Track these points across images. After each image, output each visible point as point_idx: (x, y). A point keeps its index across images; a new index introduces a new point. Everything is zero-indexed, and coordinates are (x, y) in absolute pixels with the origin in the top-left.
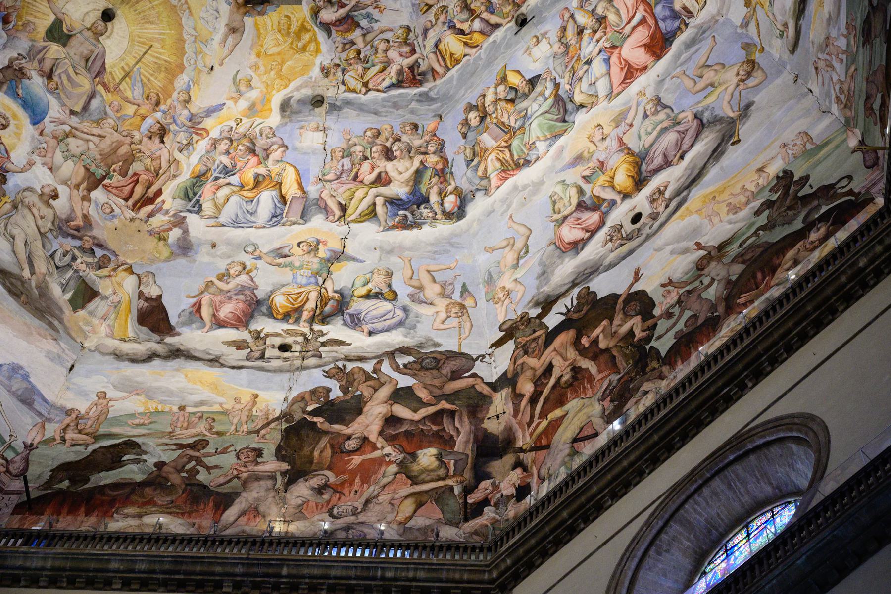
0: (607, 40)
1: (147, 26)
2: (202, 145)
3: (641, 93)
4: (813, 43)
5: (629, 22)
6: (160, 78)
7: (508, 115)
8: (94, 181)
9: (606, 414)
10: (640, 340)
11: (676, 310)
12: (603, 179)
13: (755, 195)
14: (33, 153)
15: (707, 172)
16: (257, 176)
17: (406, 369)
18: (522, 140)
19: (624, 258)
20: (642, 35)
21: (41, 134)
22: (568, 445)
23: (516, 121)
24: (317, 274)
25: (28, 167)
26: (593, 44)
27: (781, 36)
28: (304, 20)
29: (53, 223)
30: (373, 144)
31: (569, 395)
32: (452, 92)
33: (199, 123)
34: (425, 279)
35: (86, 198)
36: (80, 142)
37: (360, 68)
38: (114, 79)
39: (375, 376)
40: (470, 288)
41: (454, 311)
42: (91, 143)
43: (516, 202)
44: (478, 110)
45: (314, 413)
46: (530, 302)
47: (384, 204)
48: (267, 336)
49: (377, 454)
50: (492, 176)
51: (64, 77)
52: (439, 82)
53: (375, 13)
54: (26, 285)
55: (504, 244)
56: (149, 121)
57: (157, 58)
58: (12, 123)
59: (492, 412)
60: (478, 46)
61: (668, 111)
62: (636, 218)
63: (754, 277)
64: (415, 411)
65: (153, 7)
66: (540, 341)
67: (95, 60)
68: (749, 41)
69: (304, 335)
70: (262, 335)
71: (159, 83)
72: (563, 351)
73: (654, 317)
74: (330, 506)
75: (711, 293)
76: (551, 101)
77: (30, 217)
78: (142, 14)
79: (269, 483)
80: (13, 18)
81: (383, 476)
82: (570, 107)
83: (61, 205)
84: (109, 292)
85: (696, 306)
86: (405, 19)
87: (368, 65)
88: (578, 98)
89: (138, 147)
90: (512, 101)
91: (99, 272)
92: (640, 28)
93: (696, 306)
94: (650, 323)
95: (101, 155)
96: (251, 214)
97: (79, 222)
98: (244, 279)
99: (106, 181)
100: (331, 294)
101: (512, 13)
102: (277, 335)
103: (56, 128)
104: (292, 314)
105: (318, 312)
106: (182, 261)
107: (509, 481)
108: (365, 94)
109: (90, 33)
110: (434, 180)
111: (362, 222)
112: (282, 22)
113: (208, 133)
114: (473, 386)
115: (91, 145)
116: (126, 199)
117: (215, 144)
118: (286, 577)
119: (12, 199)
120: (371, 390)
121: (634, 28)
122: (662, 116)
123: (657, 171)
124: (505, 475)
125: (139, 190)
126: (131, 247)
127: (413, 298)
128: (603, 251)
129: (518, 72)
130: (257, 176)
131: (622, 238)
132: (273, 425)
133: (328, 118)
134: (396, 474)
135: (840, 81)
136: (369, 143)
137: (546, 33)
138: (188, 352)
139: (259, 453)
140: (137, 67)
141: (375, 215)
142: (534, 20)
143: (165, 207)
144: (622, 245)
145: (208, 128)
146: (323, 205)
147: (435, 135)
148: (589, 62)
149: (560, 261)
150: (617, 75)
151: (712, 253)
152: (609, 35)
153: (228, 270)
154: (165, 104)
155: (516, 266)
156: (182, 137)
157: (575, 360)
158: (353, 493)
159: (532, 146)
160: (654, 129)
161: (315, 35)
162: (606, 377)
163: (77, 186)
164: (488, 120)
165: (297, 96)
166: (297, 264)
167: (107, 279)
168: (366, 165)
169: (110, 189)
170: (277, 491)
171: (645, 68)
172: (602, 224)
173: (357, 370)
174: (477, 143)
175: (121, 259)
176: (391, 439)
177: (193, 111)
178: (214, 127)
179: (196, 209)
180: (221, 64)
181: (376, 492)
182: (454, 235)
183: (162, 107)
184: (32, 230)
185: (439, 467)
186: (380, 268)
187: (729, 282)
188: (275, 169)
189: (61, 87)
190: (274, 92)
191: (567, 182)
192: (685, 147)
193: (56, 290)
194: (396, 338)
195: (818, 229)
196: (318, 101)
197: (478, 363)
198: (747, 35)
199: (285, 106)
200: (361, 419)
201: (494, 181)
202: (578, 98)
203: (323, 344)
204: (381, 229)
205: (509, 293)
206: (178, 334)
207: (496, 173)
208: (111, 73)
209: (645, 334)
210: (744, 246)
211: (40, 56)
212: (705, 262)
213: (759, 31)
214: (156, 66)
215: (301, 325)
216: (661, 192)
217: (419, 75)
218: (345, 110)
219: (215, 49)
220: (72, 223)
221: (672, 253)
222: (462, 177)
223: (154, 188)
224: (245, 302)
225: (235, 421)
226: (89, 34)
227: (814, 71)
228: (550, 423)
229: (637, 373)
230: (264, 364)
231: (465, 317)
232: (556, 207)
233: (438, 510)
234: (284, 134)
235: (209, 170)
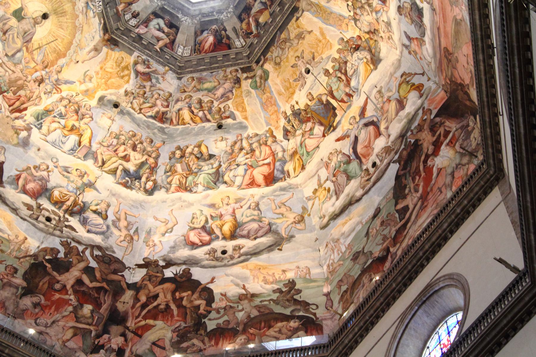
0: (251, 161)
1: (60, 29)
3: (253, 196)
4: (331, 235)
5: (263, 160)
7: (194, 165)
9: (173, 341)
10: (201, 314)
11: (222, 311)
12: (219, 222)
13: (276, 282)
15: (263, 254)
16: (73, 126)
17: (96, 258)
18: (194, 179)
19: (211, 267)
20: (265, 170)
22: (150, 344)
23: (195, 168)
24: (78, 188)
26: (244, 158)
27: (320, 218)
28: (129, 64)
30: (130, 139)
31: (160, 317)
32: (175, 135)
33: (60, 85)
34: (123, 216)
36: (3, 70)
37: (142, 100)
38: (33, 47)
39: (82, 254)
40: (139, 231)
41: (128, 238)
42: (7, 73)
43: (178, 205)
44: (182, 152)
45: (48, 261)
46: (161, 257)
47: (122, 171)
48: (44, 209)
49: (67, 297)
50: (173, 185)
51: (11, 36)
52: (171, 127)
53: (161, 79)
55: (164, 220)
57: (57, 46)
59: (122, 300)
60: (196, 123)
61: (259, 212)
62: (224, 252)
63: (261, 324)
64: (91, 282)
66: (158, 279)
68: (306, 207)
69: (60, 217)
70: (41, 207)
71: (51, 58)
72: (166, 292)
73: (211, 307)
74: (37, 317)
75: (240, 315)
76: (214, 170)
79: (15, 290)
81: (65, 311)
82: (221, 179)
85: (231, 318)
86: (171, 90)
87: (146, 101)
88: (226, 178)
89: (27, 83)
90: (198, 158)
92: (266, 166)
93: (231, 318)
94: (209, 308)
96: (63, 143)
98: (45, 174)
99: (5, 94)
100: (80, 202)
101: (218, 120)
102: (48, 211)
104: (58, 203)
105: (70, 208)
106: (21, 150)
107: (116, 342)
108: (138, 114)
110: (148, 171)
111: (109, 174)
113: (61, 91)
114: (120, 281)
116: (10, 106)
117: (62, 99)
118: (6, 354)
120: (77, 261)
121: (264, 164)
122: (256, 213)
123: (243, 237)
124: (116, 336)
125: (18, 104)
127: (113, 222)
128: (203, 257)
129: (207, 148)
130: (73, 126)
131: (214, 257)
132: (28, 258)
133: (117, 116)
134: (71, 312)
135: (333, 260)
136: (129, 138)
137: (227, 139)
138: (5, 198)
139: (16, 271)
141: (116, 174)
142: (225, 130)
143: (25, 118)
144: (213, 260)
145: (62, 90)
146: (95, 156)
147: (158, 150)
148: (238, 165)
149: (183, 247)
150: (247, 181)
151: (248, 296)
152: (252, 160)
153: (40, 165)
155: (163, 235)
156: (49, 88)
157: (169, 301)
158: (49, 314)
159: (196, 185)
160: (250, 216)
161: (130, 73)
162: (180, 321)
164: (184, 159)
165: (109, 97)
166: (72, 179)
168: (122, 148)
170: (17, 297)
171: (259, 186)
172: (208, 243)
173: (75, 248)
174: (174, 166)
176: (76, 292)
177: (60, 77)
178: (66, 90)
179: (39, 127)
180: (83, 62)
181: (59, 318)
182: (144, 201)
183: (47, 70)
185: (90, 318)
186: (107, 201)
187: (249, 316)
188: (83, 127)
190: (100, 90)
191: (203, 212)
192: (259, 235)
194: (98, 239)
195: (295, 322)
196: (116, 106)
197: (127, 270)
198: (306, 204)
199: (101, 99)
200: (67, 274)
201: (173, 189)
202: (226, 178)
203: (66, 226)
204: (115, 181)
205: (155, 245)
206: (4, 187)
207: (175, 185)
209: (204, 312)
210: (263, 303)
211: (5, 22)
212: (243, 297)
213: (312, 207)
215: (61, 211)
216: (240, 249)
217: (165, 118)
218: (126, 116)
219: (83, 54)
221: (232, 281)
222: (160, 176)
223: (24, 106)
224: (41, 186)
225: (12, 247)
226: (32, 21)
227: (325, 245)
228: (146, 324)
229: (193, 331)
230: (36, 223)
231: (131, 244)
232: (193, 220)
233: (81, 342)
234: (94, 112)
235: (53, 110)
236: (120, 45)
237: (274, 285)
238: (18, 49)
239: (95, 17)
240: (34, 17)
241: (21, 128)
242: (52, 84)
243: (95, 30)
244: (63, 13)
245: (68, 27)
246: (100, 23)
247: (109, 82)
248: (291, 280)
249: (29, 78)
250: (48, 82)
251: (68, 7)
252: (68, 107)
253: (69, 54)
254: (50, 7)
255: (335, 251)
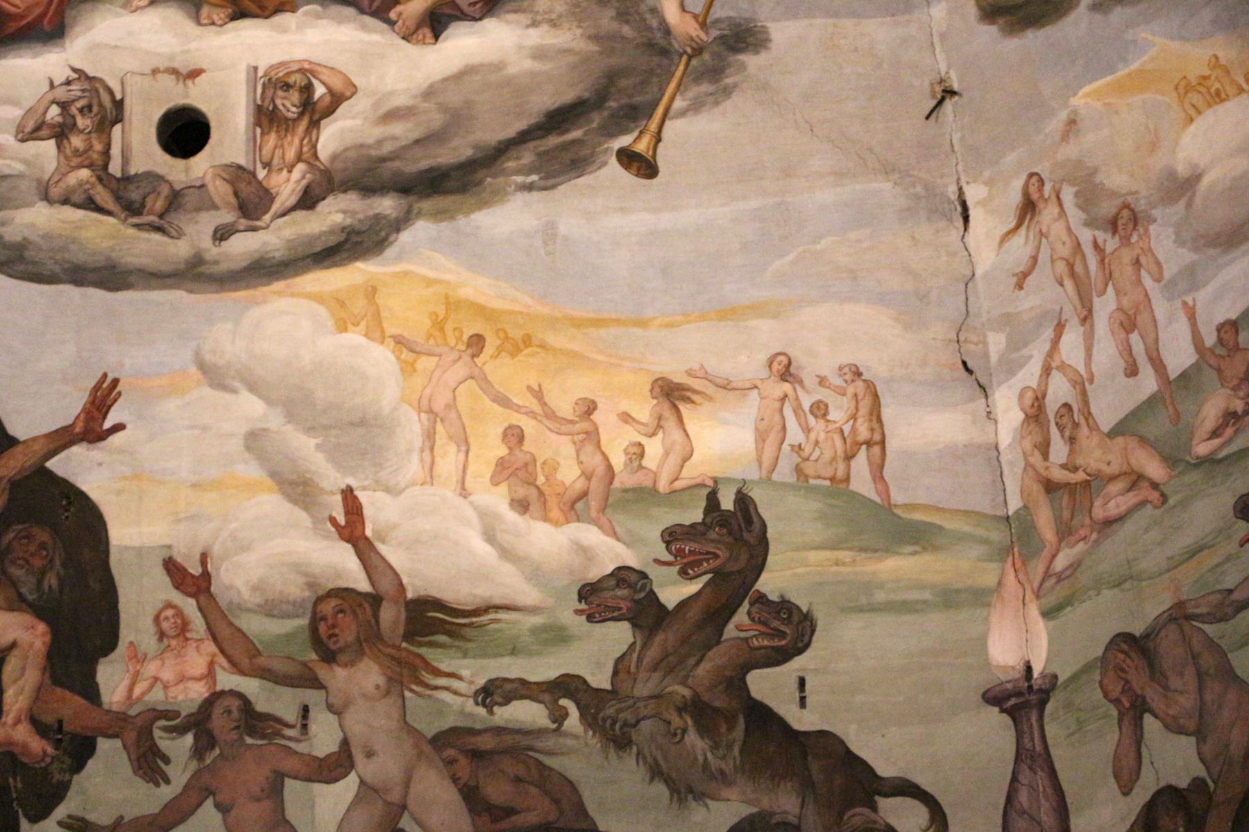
11: (179, 748)
73: (91, 693)
94: (69, 706)
131: (101, 169)
135: (1081, 385)
144: (90, 204)
151: (389, 615)
212: (348, 633)
221: (255, 440)
227: (1014, 196)
237: (591, 535)
248: (727, 502)
255: (1105, 306)
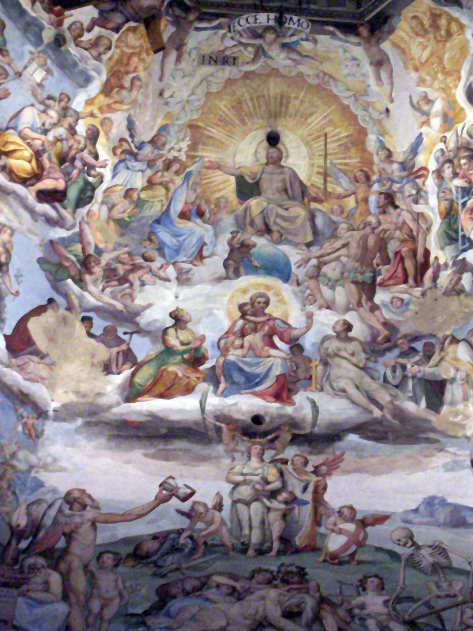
1: (309, 120)
2: (430, 183)
6: (353, 155)
8: (368, 289)
14: (305, 306)
21: (298, 284)
25: (310, 321)
28: (431, 10)
29: (364, 351)
33: (413, 166)
35: (374, 308)
36: (333, 264)
38: (318, 188)
51: (279, 221)
54: (384, 423)
56: (373, 199)
57: (338, 140)
58: (270, 294)
65: (302, 101)
67: (291, 186)
71: (355, 160)
77: (344, 363)
78: (299, 114)
80: (204, 207)
83: (359, 331)
84: (452, 373)
89: (381, 228)
91: (432, 362)
95: (357, 261)
97: (384, 332)
99: (379, 279)
103: (306, 269)
109: (271, 166)
112: (413, 25)
115: (344, 259)
117: (439, 173)
119: (318, 358)
125: (409, 265)
126: (440, 319)
140: (328, 161)
143: (442, 261)
145: (423, 165)
154: (374, 173)
156: (409, 190)
161: (447, 13)
163: (359, 304)
167: (444, 363)
169: (387, 283)
175: (440, 335)
178: (428, 160)
179: (467, 245)
180: (392, 101)
183: (374, 178)
184: (354, 372)
189: (283, 232)
190: (453, 91)
193: (410, 407)
208: (312, 185)
211: (248, 220)
214: (342, 148)
220: (380, 339)
223: (420, 252)
226: (270, 168)
235: (452, 202)
236: (390, 12)
238: (308, 216)
239: (315, 42)
240: (265, 161)
241: (456, 279)
242: (404, 181)
243: (341, 51)
244: (283, 102)
245: (311, 102)
246: (332, 34)
247: (448, 66)
249: (372, 219)
250: (398, 185)
251: (274, 88)
252: (458, 171)
253: (365, 120)
254: (260, 121)
